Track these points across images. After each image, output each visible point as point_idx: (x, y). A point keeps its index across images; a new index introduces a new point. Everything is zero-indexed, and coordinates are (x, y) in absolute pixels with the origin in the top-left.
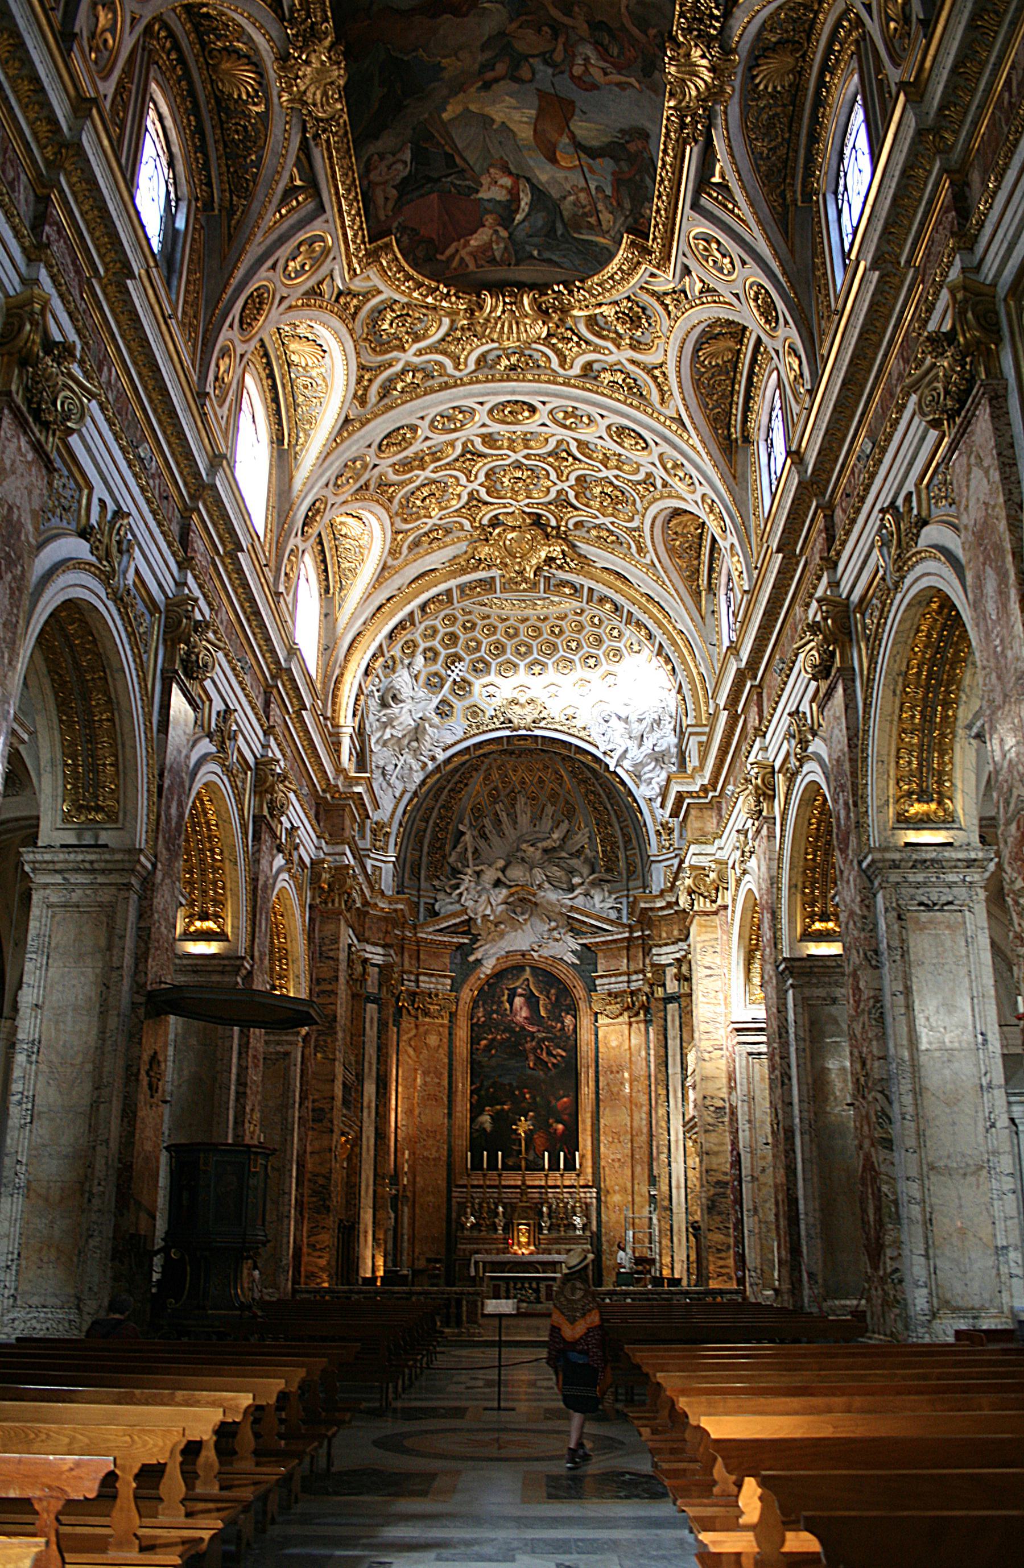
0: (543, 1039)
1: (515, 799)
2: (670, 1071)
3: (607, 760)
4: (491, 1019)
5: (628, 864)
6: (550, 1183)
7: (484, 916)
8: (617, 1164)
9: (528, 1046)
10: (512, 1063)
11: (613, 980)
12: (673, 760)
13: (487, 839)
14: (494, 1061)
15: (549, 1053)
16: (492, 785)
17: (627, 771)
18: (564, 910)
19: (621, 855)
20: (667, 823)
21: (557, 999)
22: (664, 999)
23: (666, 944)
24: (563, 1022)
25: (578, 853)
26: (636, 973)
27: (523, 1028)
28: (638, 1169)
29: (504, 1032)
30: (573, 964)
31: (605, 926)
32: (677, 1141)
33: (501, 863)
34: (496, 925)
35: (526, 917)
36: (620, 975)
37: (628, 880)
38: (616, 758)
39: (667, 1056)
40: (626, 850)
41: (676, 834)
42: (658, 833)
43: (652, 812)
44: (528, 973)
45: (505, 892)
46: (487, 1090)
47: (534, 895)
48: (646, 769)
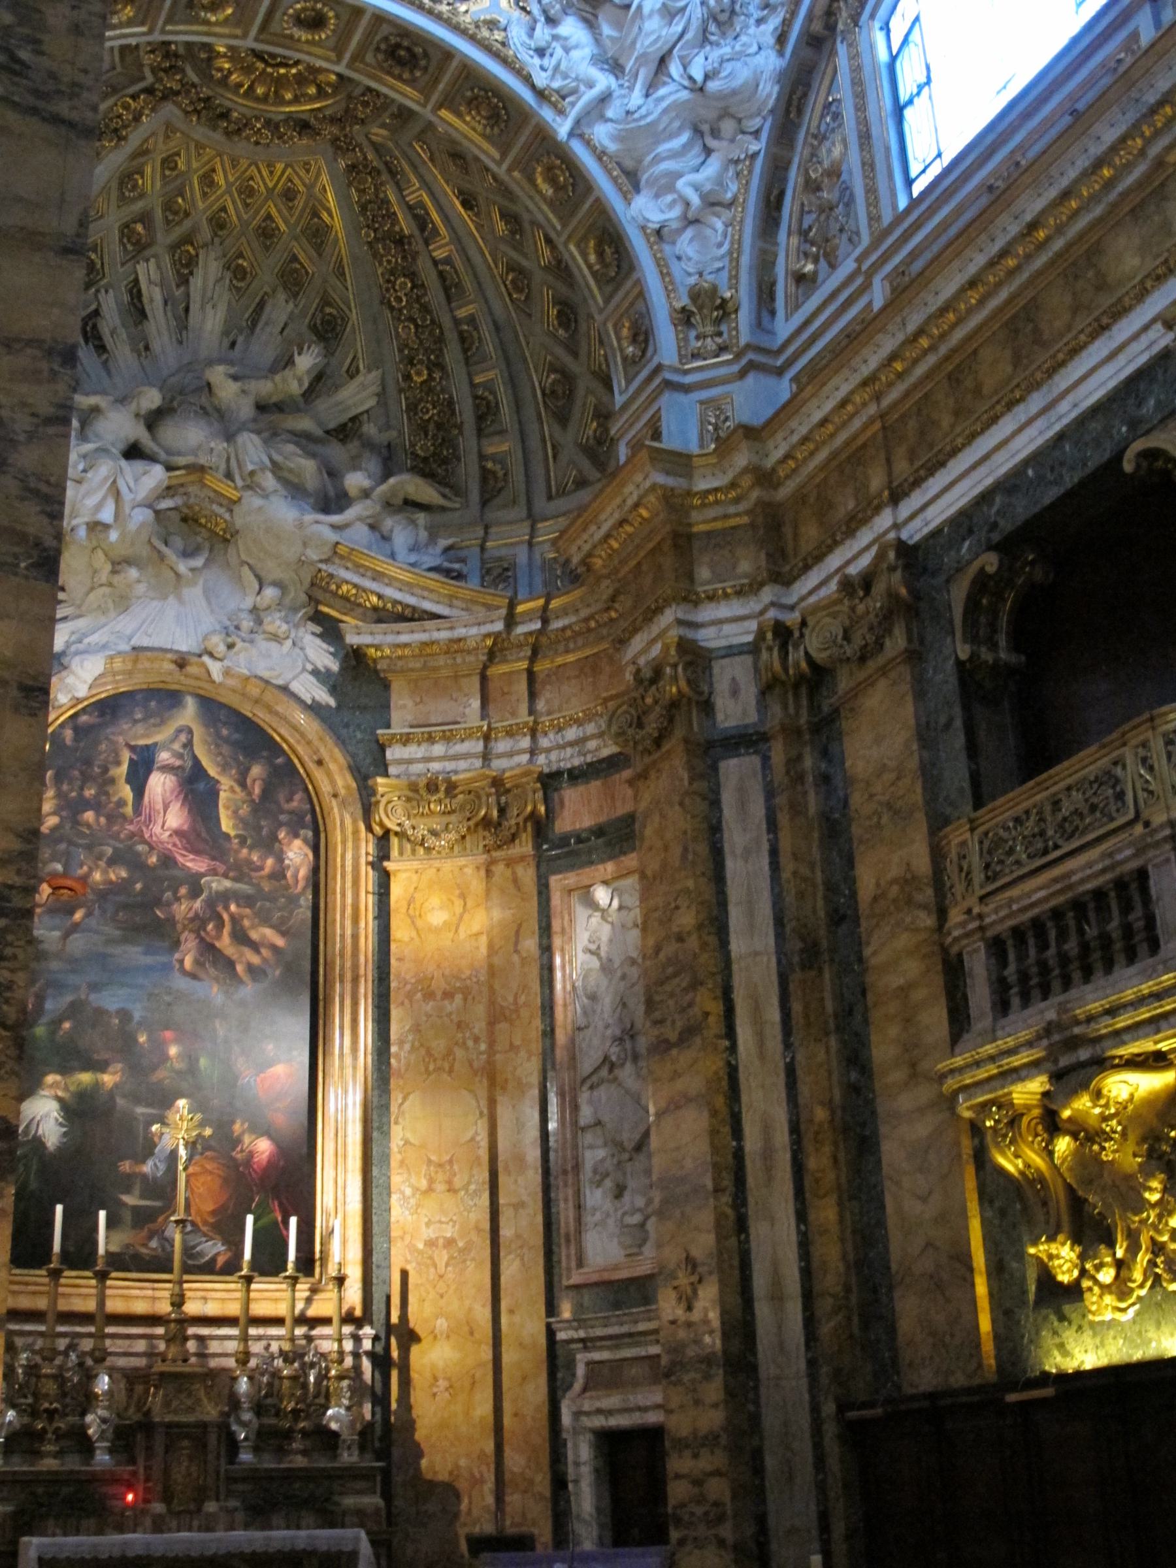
0: (225, 897)
1: (191, 263)
2: (737, 946)
3: (547, 114)
4: (76, 823)
5: (485, 475)
6: (260, 1309)
7: (96, 527)
8: (442, 1257)
9: (183, 909)
10: (134, 954)
11: (438, 749)
12: (756, 123)
13: (101, 348)
14: (78, 944)
15: (241, 937)
16: (139, 206)
17: (600, 155)
18: (313, 555)
19: (468, 442)
20: (714, 289)
21: (266, 793)
22: (710, 745)
23: (711, 598)
24: (280, 859)
25: (345, 432)
26: (510, 733)
27: (167, 860)
28: (510, 1269)
29: (112, 862)
30: (314, 709)
31: (428, 606)
32: (768, 1153)
33: (152, 399)
34: (118, 564)
35: (198, 562)
36: (469, 735)
37: (484, 503)
38: (573, 114)
39: (723, 904)
40: (480, 432)
41: (744, 317)
42: (684, 318)
43: (662, 266)
44: (188, 714)
45: (155, 476)
46: (57, 1023)
47: (231, 505)
48: (664, 148)
